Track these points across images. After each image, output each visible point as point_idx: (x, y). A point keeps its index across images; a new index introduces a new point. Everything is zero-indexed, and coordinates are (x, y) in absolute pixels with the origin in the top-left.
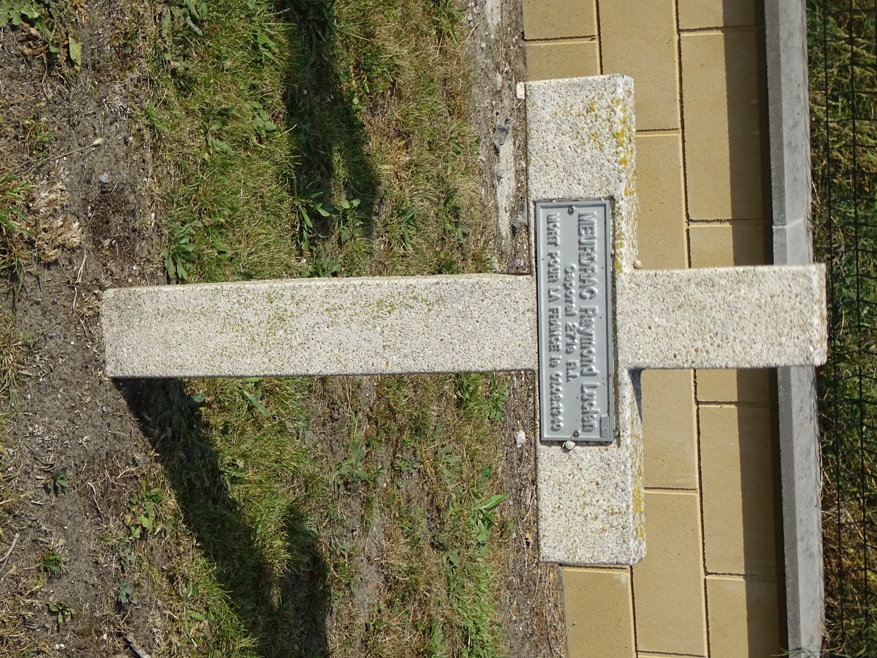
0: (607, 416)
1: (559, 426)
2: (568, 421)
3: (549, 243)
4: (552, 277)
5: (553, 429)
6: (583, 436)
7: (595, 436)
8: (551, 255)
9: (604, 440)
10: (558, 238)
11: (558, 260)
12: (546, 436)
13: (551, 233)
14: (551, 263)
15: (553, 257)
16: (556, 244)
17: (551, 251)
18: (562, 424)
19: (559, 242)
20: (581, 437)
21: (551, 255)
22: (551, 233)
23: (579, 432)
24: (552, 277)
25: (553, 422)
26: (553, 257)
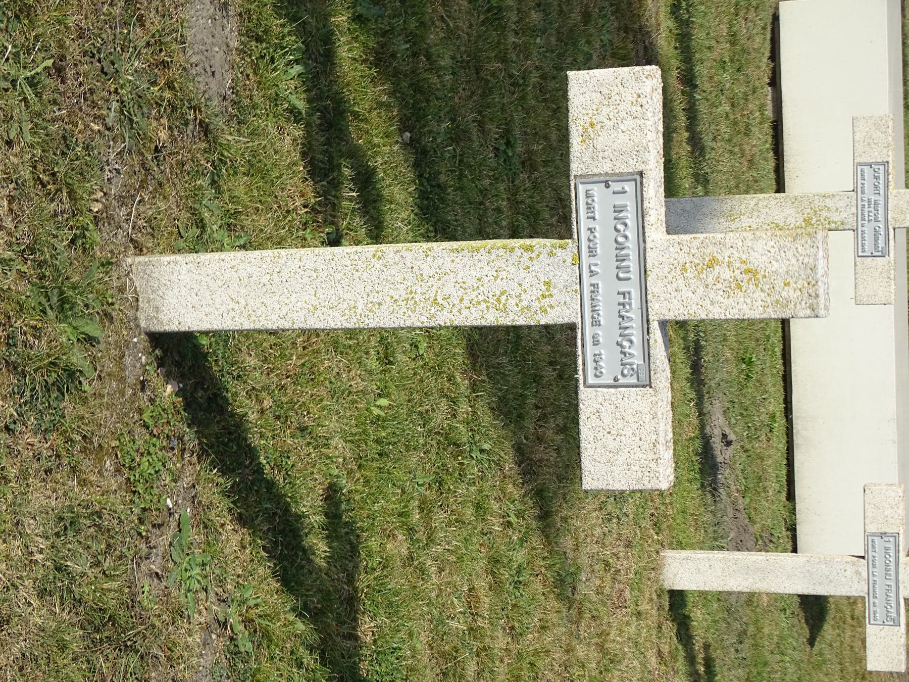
0: (642, 362)
1: (601, 373)
2: (609, 368)
3: (588, 218)
4: (592, 252)
5: (596, 376)
6: (622, 381)
7: (633, 380)
8: (590, 229)
9: (639, 383)
10: (596, 213)
11: (596, 234)
12: (591, 380)
13: (590, 208)
14: (591, 238)
15: (592, 232)
16: (594, 219)
17: (590, 226)
18: (603, 370)
19: (597, 217)
20: (620, 381)
21: (590, 229)
22: (590, 208)
23: (619, 377)
24: (592, 252)
25: (596, 369)
26: (592, 232)
